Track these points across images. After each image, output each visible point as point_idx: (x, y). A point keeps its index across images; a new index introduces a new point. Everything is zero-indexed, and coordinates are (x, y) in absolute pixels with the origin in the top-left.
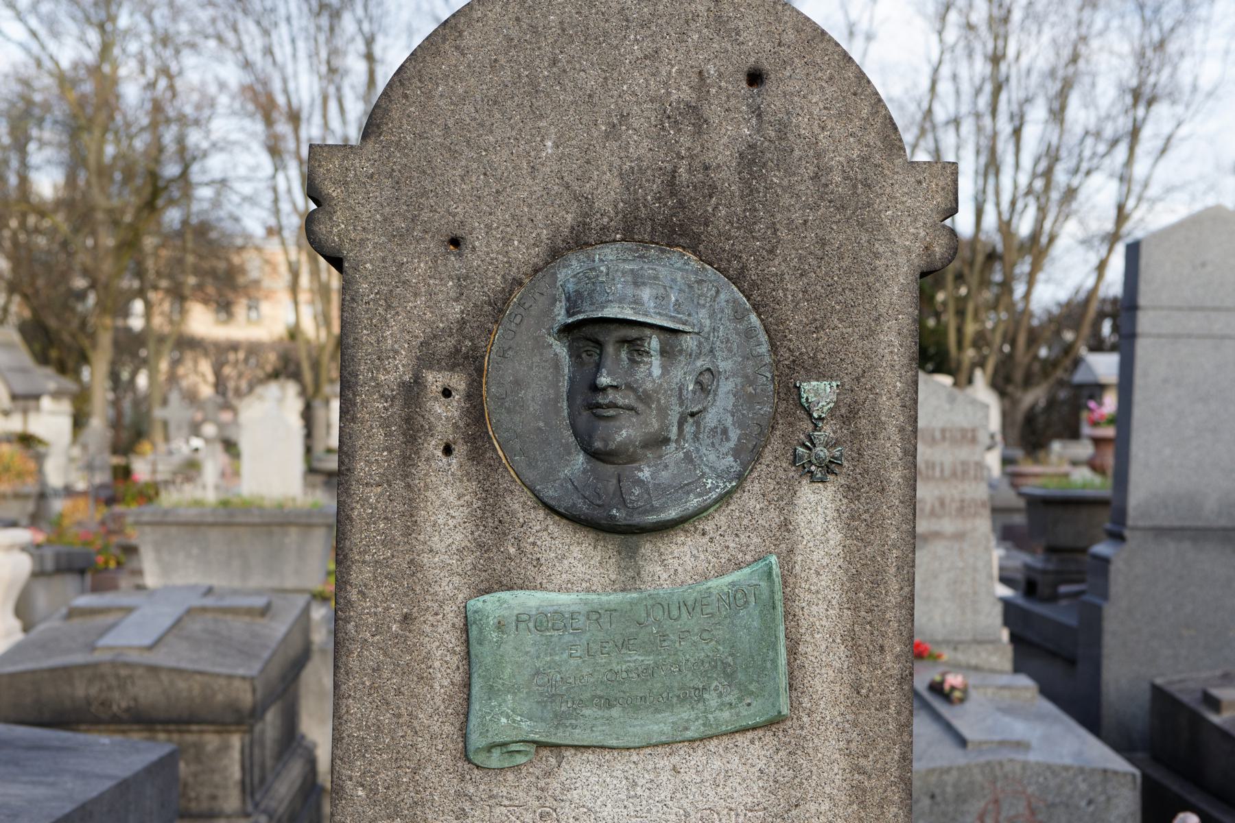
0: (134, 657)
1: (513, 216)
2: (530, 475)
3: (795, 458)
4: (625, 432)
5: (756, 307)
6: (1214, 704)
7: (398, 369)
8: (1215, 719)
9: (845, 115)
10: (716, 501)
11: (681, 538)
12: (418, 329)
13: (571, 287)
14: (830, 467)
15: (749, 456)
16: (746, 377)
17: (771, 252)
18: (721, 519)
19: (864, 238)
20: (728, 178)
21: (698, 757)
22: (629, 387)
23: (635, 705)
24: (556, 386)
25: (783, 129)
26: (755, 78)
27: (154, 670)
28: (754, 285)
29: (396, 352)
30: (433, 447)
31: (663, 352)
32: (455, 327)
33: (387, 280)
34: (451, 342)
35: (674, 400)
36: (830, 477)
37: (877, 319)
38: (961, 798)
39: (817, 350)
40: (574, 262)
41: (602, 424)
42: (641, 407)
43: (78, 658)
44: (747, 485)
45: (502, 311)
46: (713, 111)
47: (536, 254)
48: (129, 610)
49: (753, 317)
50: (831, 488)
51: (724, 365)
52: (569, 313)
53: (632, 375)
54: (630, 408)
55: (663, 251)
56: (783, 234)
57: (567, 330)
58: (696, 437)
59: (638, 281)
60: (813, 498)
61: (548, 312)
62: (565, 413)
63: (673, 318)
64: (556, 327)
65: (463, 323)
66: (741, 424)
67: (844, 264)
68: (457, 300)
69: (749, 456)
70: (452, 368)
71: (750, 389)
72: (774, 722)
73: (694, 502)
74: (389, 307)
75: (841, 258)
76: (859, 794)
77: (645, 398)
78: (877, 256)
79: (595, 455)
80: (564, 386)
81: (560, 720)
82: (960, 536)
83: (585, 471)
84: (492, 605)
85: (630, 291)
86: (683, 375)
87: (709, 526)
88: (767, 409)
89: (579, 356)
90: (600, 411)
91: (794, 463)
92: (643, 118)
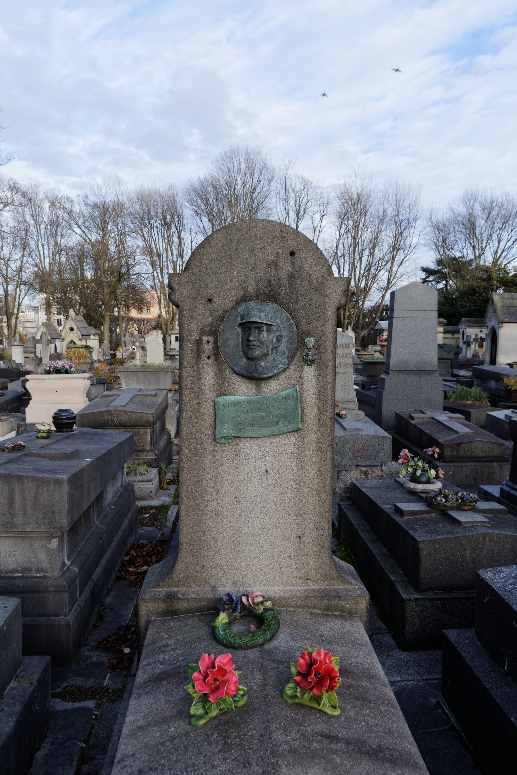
0: (120, 408)
1: (226, 293)
2: (231, 364)
3: (303, 359)
4: (257, 353)
5: (293, 318)
6: (412, 418)
7: (195, 336)
8: (412, 422)
9: (317, 264)
10: (282, 371)
11: (272, 381)
12: (200, 325)
13: (242, 313)
14: (313, 362)
15: (291, 359)
16: (290, 337)
17: (297, 302)
18: (283, 376)
19: (322, 298)
20: (285, 282)
21: (277, 440)
22: (258, 340)
23: (260, 426)
24: (238, 340)
25: (300, 268)
26: (292, 254)
27: (126, 412)
28: (292, 312)
29: (194, 331)
30: (205, 357)
31: (267, 331)
32: (210, 324)
33: (191, 311)
34: (209, 328)
35: (270, 344)
36: (313, 364)
37: (326, 321)
38: (344, 444)
39: (309, 330)
40: (243, 306)
41: (251, 350)
42: (261, 346)
43: (105, 409)
44: (290, 367)
45: (223, 319)
46: (281, 263)
47: (232, 304)
48: (118, 395)
49: (292, 321)
50: (313, 367)
51: (283, 334)
52: (241, 320)
53: (259, 337)
54: (258, 346)
55: (267, 303)
56: (300, 297)
57: (241, 325)
58: (276, 354)
59: (260, 311)
60: (308, 370)
61: (236, 320)
62: (241, 347)
63: (270, 321)
64: (238, 324)
65: (212, 323)
66: (288, 350)
67: (317, 306)
68: (210, 316)
69: (291, 359)
70: (209, 335)
71: (291, 341)
72: (298, 430)
73: (276, 371)
74: (192, 319)
75: (316, 304)
76: (320, 449)
77: (263, 343)
78: (326, 303)
79: (249, 359)
80: (240, 340)
81: (240, 430)
82: (345, 373)
83: (246, 363)
84: (222, 400)
85: (258, 314)
86: (273, 337)
87: (280, 378)
88: (296, 346)
89: (244, 332)
90: (250, 347)
91: (303, 361)
92: (261, 265)
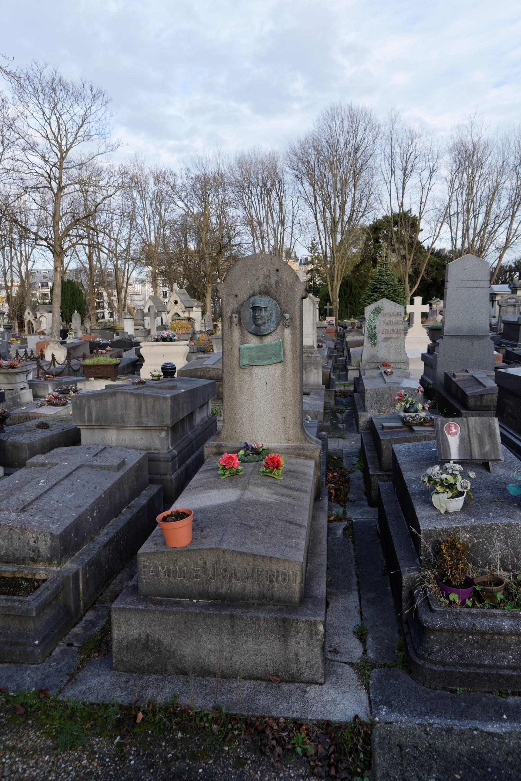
0: (210, 366)
4: (260, 322)
6: (454, 376)
7: (229, 314)
8: (454, 379)
9: (290, 276)
14: (289, 326)
15: (278, 325)
18: (274, 334)
20: (274, 285)
21: (271, 367)
23: (262, 360)
25: (281, 278)
26: (277, 270)
27: (214, 369)
30: (234, 325)
38: (383, 394)
43: (199, 367)
46: (271, 276)
47: (247, 297)
48: (209, 357)
51: (274, 312)
57: (252, 308)
59: (261, 301)
69: (278, 325)
72: (281, 362)
76: (294, 372)
77: (262, 317)
79: (256, 325)
81: (252, 362)
82: (397, 338)
84: (242, 346)
86: (268, 314)
92: (261, 277)
